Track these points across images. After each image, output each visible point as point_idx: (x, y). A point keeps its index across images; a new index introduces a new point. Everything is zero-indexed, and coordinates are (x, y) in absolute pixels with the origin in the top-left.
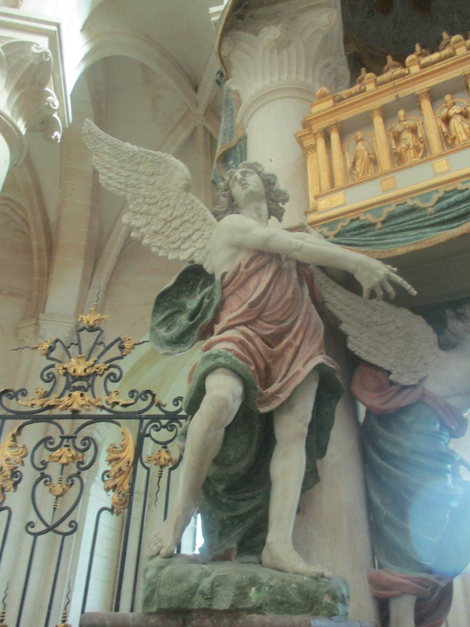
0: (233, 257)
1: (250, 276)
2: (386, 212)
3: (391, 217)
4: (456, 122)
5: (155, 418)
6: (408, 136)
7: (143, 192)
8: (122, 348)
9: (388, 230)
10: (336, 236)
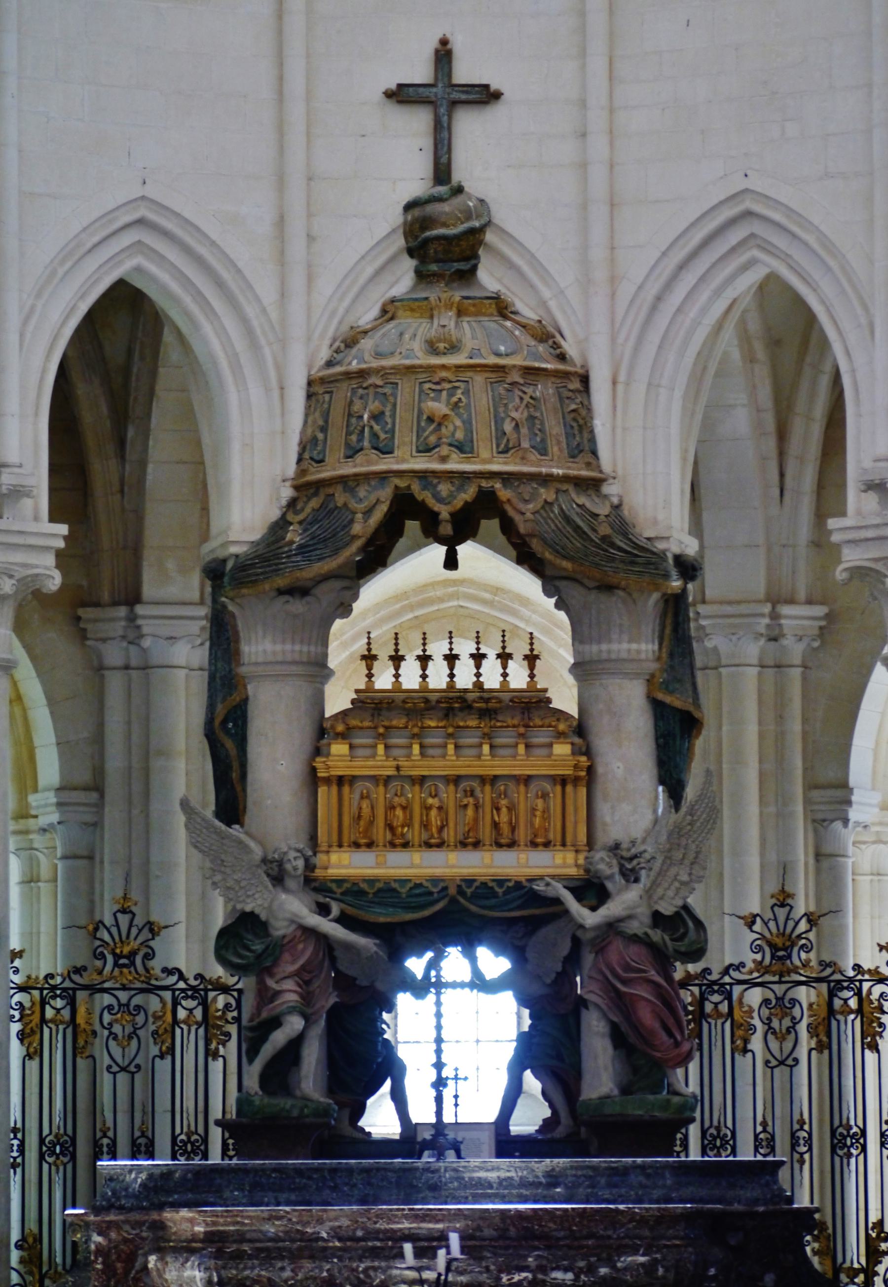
0: (289, 926)
1: (300, 942)
2: (379, 885)
3: (380, 890)
4: (434, 813)
5: (183, 990)
6: (399, 812)
7: (223, 857)
8: (151, 930)
9: (376, 900)
10: (342, 894)
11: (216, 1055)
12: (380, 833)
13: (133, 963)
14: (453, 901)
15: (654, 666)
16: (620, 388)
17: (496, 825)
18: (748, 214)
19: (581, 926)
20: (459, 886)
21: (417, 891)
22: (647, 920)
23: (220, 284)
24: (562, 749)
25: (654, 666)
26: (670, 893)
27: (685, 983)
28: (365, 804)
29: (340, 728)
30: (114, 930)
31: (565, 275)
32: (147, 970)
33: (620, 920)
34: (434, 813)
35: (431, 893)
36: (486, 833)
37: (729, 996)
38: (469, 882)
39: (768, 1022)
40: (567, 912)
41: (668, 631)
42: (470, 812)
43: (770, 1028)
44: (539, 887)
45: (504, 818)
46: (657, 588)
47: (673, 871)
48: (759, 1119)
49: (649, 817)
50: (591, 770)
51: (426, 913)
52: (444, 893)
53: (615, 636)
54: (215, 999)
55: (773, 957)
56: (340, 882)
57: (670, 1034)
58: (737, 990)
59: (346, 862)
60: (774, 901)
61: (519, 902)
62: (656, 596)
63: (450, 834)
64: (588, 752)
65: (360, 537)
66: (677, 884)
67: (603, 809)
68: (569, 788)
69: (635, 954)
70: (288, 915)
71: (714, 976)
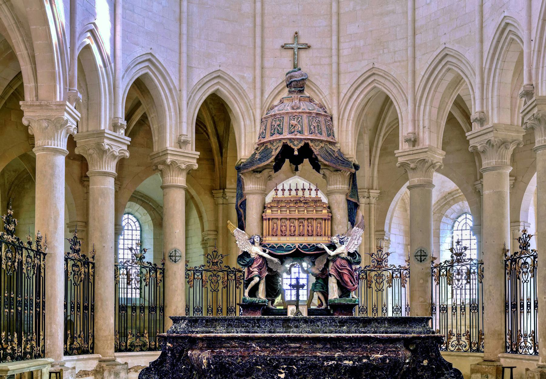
4: (292, 227)
6: (284, 227)
11: (238, 288)
12: (279, 233)
15: (348, 191)
16: (340, 121)
17: (308, 231)
19: (330, 256)
22: (346, 254)
23: (239, 94)
24: (325, 211)
25: (348, 191)
26: (352, 247)
27: (355, 270)
28: (275, 225)
29: (269, 206)
31: (326, 92)
34: (292, 227)
36: (306, 233)
37: (366, 274)
40: (326, 252)
41: (351, 182)
42: (301, 227)
44: (319, 246)
45: (310, 228)
46: (349, 171)
47: (353, 241)
49: (346, 229)
50: (331, 217)
51: (290, 252)
53: (338, 184)
56: (269, 245)
57: (352, 283)
58: (368, 272)
62: (349, 173)
63: (297, 233)
64: (331, 213)
67: (335, 227)
68: (326, 221)
69: (344, 262)
71: (362, 269)
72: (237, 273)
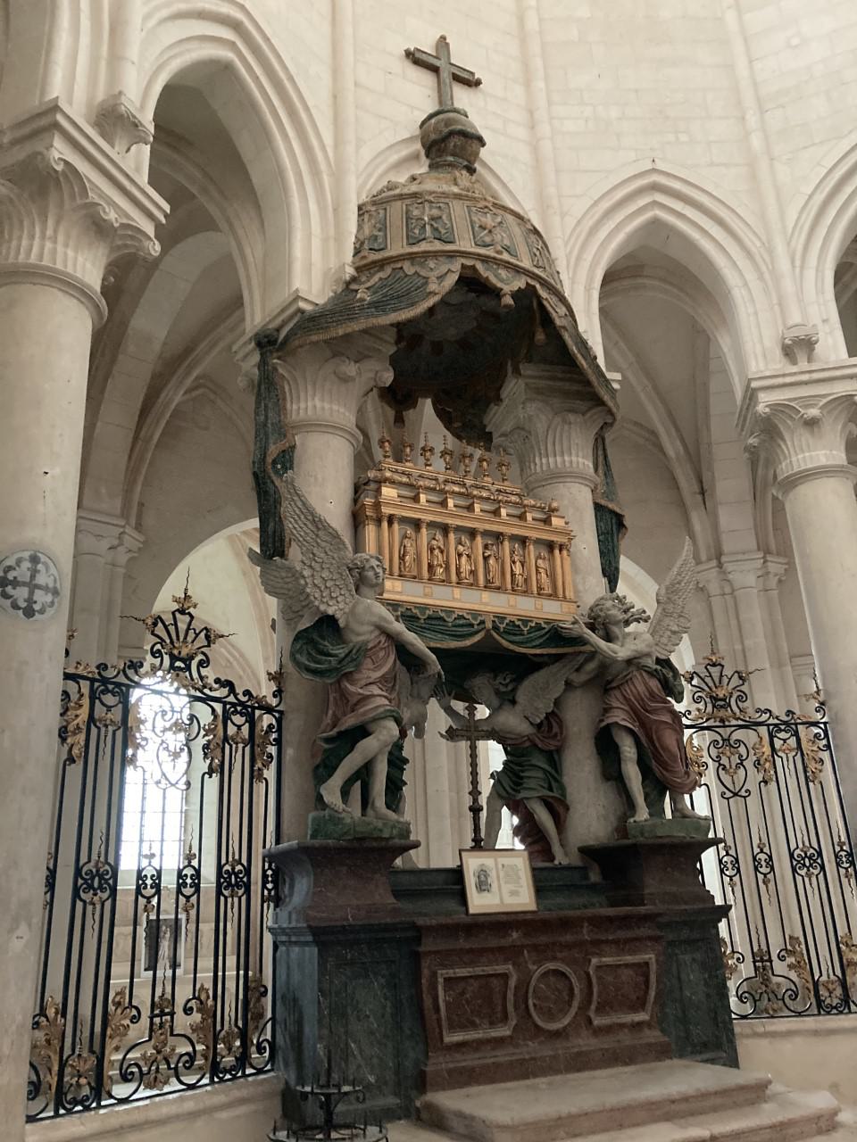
3: (429, 618)
4: (464, 559)
9: (427, 626)
13: (188, 668)
14: (488, 631)
18: (655, 187)
20: (494, 621)
21: (461, 622)
30: (172, 629)
32: (201, 678)
33: (635, 658)
34: (464, 559)
35: (472, 625)
38: (501, 618)
39: (718, 760)
43: (720, 765)
45: (518, 569)
48: (756, 842)
51: (468, 643)
52: (482, 626)
54: (261, 716)
55: (714, 706)
59: (399, 590)
60: (707, 662)
61: (541, 641)
65: (436, 294)
66: (669, 633)
70: (374, 619)
72: (257, 713)
